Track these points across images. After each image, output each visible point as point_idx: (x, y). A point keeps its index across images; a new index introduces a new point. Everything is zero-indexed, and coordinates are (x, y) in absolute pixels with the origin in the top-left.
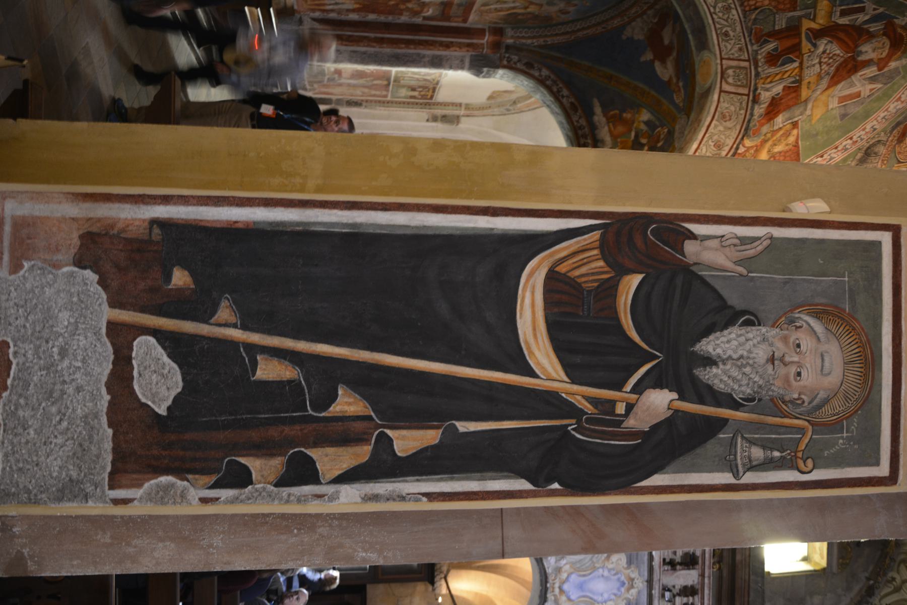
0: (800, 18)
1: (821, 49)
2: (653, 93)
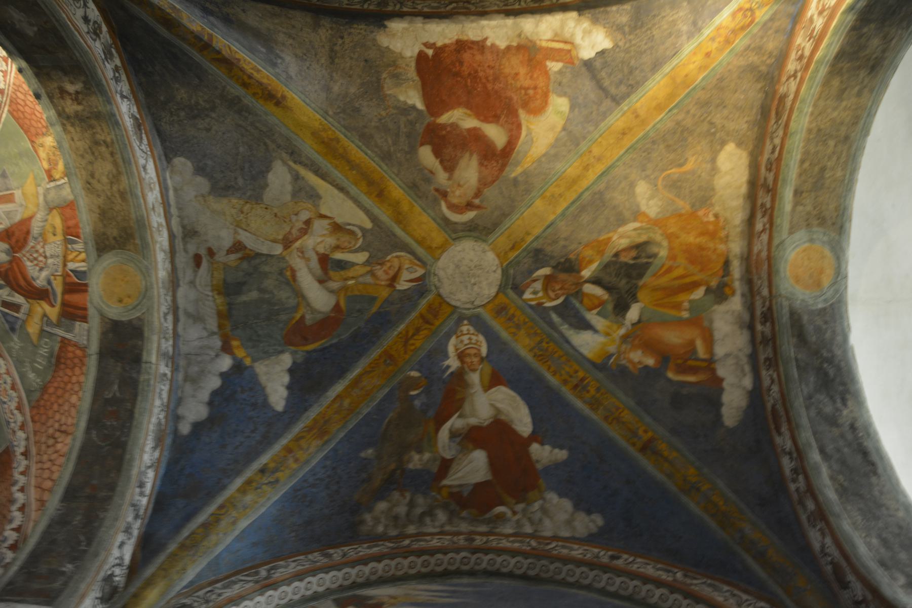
0: (58, 325)
1: (44, 274)
2: (553, 381)
